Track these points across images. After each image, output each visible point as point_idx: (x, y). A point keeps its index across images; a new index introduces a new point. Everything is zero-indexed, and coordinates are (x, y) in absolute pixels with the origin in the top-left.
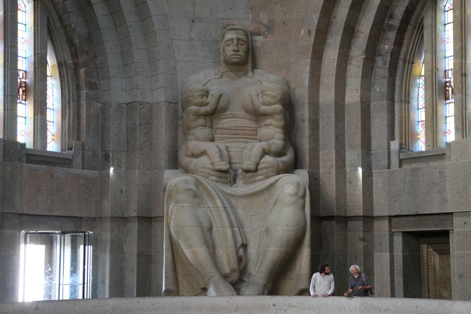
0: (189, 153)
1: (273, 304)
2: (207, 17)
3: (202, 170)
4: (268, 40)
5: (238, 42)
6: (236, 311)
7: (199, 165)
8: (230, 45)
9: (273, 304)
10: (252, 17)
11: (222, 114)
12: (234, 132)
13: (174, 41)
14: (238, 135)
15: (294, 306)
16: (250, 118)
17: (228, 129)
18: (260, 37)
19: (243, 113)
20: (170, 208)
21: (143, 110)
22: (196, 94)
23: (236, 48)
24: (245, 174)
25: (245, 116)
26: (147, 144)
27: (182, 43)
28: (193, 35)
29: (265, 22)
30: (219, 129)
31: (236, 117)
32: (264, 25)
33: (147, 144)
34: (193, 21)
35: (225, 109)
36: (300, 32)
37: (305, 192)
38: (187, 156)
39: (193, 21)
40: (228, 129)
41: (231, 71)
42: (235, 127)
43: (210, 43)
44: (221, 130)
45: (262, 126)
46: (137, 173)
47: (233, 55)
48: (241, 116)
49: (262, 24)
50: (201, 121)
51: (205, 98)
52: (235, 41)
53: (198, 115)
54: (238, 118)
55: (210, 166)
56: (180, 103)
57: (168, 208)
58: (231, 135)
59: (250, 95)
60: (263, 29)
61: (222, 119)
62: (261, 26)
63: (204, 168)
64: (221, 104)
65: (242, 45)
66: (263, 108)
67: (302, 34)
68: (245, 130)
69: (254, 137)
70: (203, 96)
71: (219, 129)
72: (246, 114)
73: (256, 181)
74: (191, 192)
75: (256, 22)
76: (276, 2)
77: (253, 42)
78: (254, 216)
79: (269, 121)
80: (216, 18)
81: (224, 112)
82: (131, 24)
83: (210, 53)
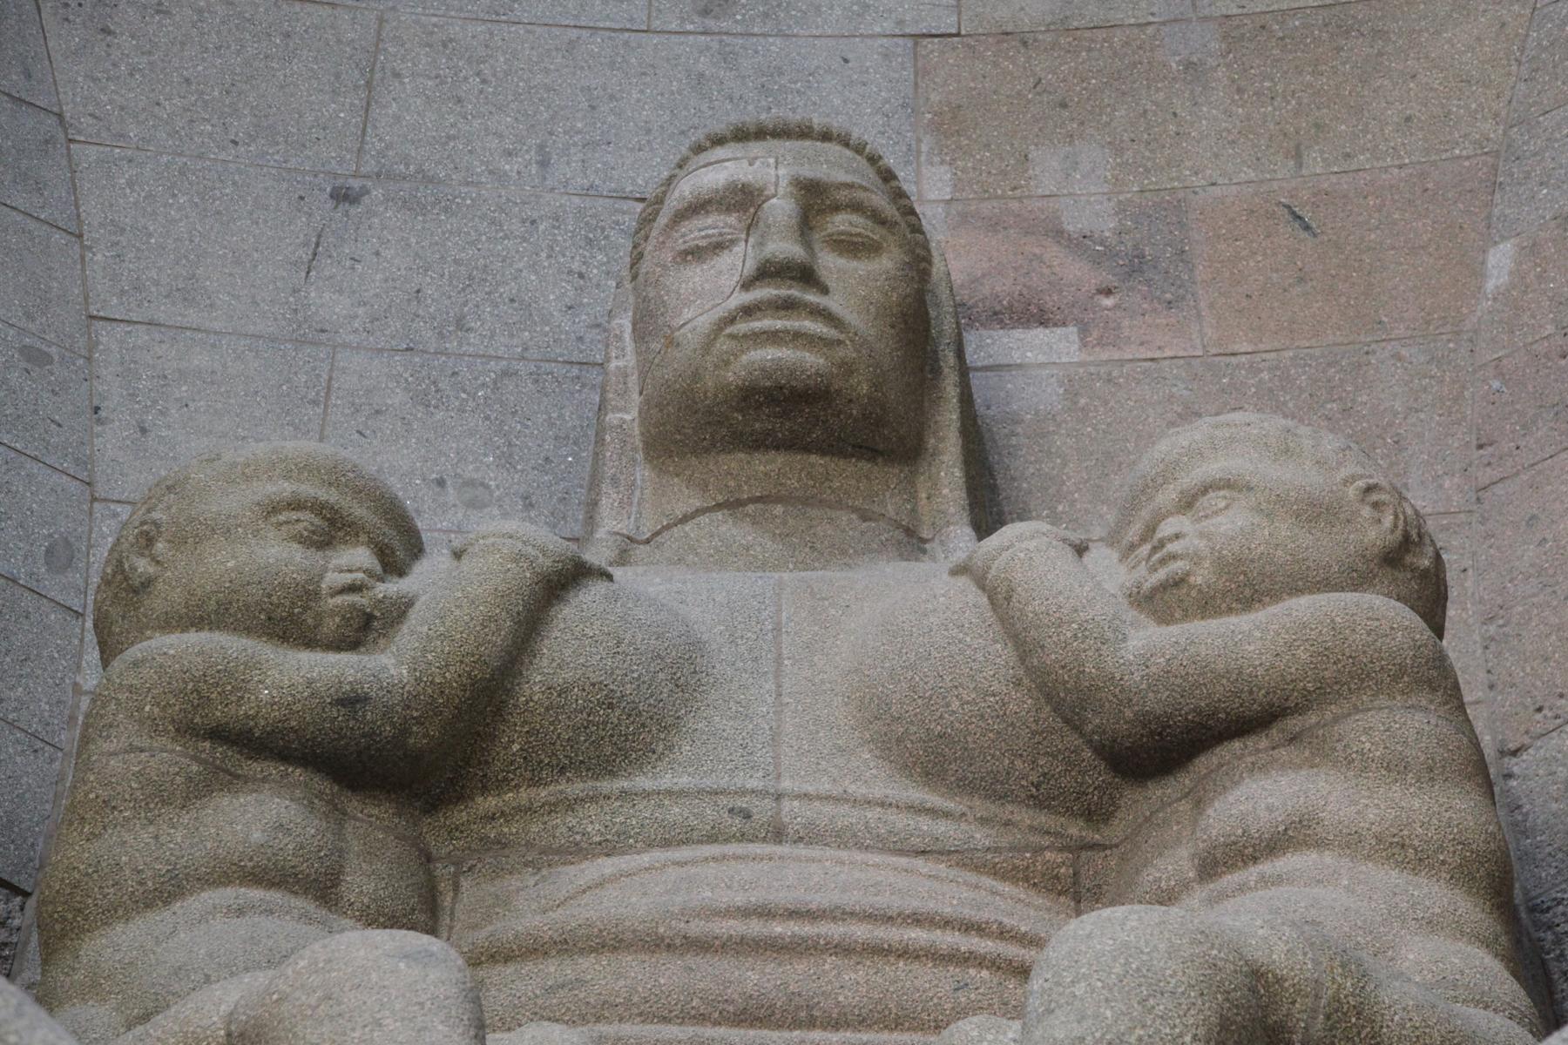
2: (499, 176)
5: (806, 224)
8: (719, 247)
10: (957, 185)
11: (576, 788)
12: (755, 978)
13: (107, 336)
16: (982, 837)
17: (654, 944)
18: (1039, 335)
19: (878, 781)
22: (236, 501)
23: (785, 247)
25: (901, 821)
28: (330, 304)
30: (534, 949)
31: (778, 834)
32: (1080, 244)
35: (617, 734)
36: (1478, 272)
40: (654, 944)
41: (732, 505)
43: (505, 373)
44: (553, 969)
47: (748, 311)
48: (847, 816)
49: (1059, 234)
50: (266, 813)
51: (357, 557)
52: (781, 208)
53: (241, 742)
54: (810, 836)
58: (702, 1019)
60: (1077, 272)
61: (578, 851)
62: (1054, 253)
64: (577, 642)
65: (850, 246)
66: (1148, 653)
68: (906, 953)
70: (331, 528)
71: (534, 949)
72: (917, 794)
75: (994, 225)
77: (976, 380)
79: (1255, 791)
80: (589, 192)
81: (606, 767)
83: (507, 461)
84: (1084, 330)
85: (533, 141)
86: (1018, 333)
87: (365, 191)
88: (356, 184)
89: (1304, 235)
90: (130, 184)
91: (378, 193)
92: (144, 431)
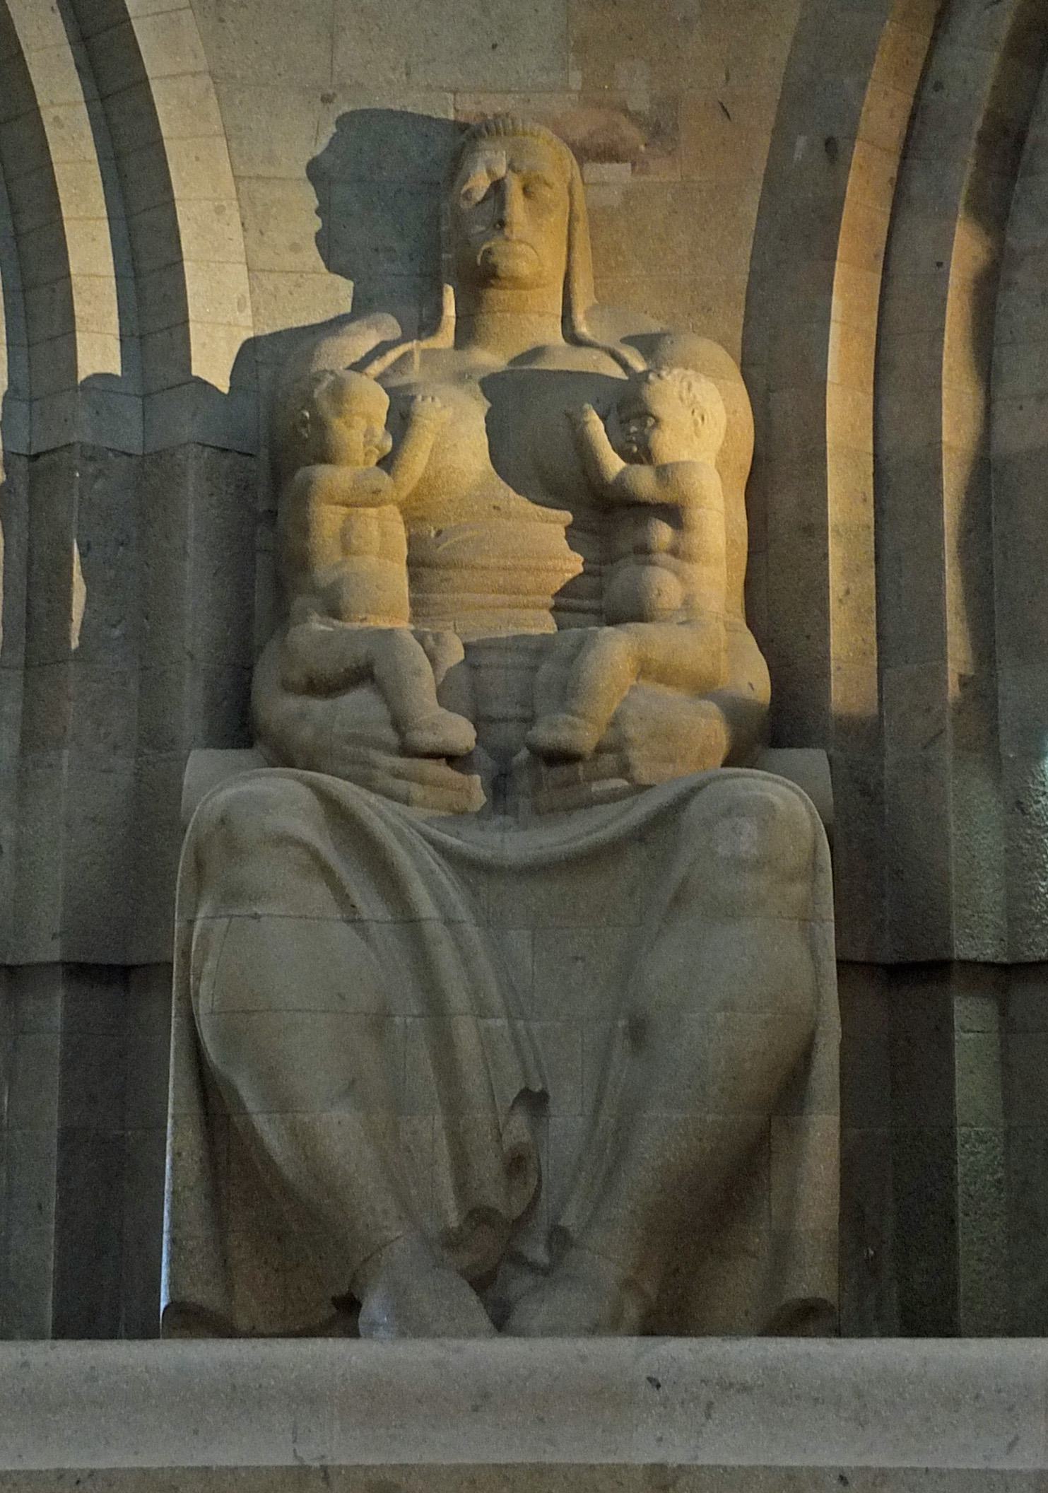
0: (296, 675)
1: (650, 1379)
2: (390, 82)
3: (349, 749)
6: (476, 1409)
7: (337, 728)
9: (650, 1379)
10: (585, 81)
14: (517, 591)
15: (745, 1389)
20: (198, 924)
21: (98, 486)
24: (543, 769)
26: (117, 632)
29: (640, 102)
32: (634, 117)
33: (117, 632)
34: (326, 99)
36: (793, 145)
37: (815, 850)
38: (288, 687)
39: (326, 99)
45: (622, 556)
46: (65, 762)
49: (625, 111)
55: (388, 735)
56: (264, 454)
57: (191, 922)
59: (568, 415)
60: (632, 134)
62: (623, 120)
63: (354, 739)
67: (797, 156)
69: (587, 603)
73: (590, 803)
74: (294, 852)
75: (599, 105)
76: (685, 19)
78: (579, 963)
82: (60, 112)
84: (634, 165)
85: (403, 61)
86: (607, 165)
88: (330, 91)
89: (726, 119)
90: (241, 103)
91: (340, 96)
92: (262, 233)
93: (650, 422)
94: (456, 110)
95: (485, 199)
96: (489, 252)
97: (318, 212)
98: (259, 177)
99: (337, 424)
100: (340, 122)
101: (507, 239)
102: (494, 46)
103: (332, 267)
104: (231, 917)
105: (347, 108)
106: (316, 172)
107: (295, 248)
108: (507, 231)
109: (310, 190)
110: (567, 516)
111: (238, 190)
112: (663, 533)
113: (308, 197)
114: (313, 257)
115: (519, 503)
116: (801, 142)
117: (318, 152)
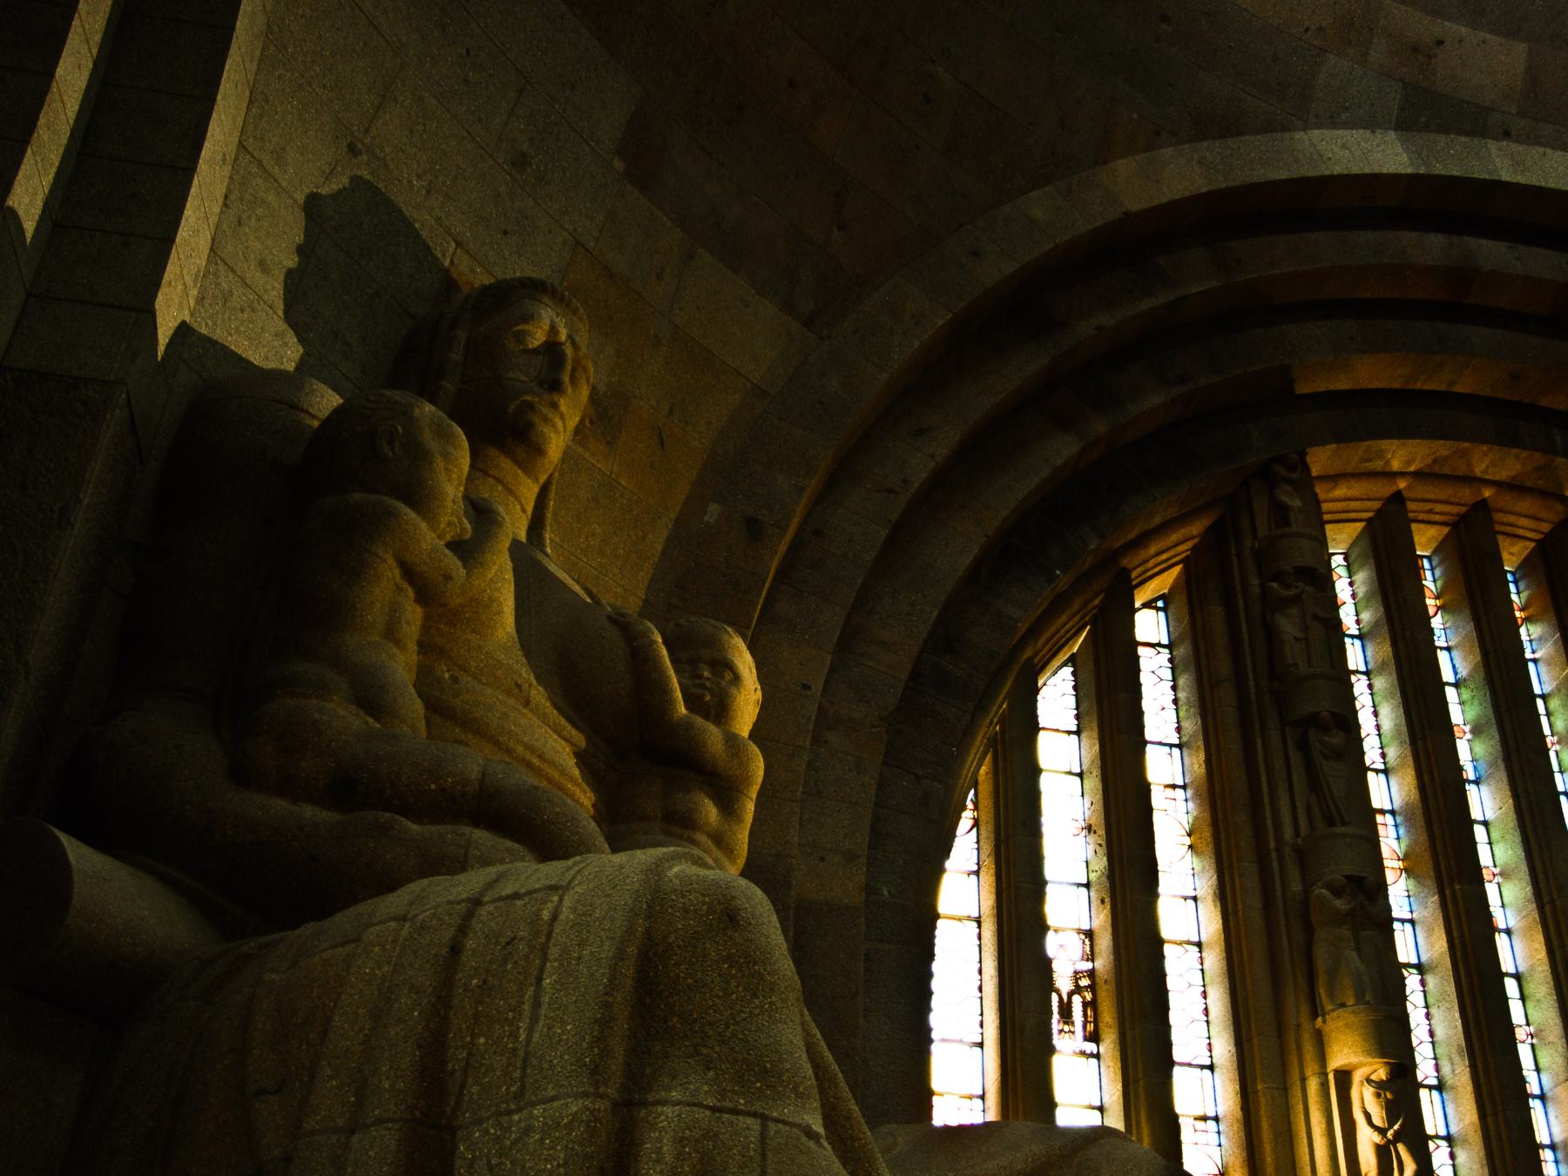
4: (587, 455)
27: (271, 198)
34: (353, 150)
42: (530, 748)
87: (360, 153)
88: (360, 146)
93: (728, 676)
94: (452, 262)
95: (535, 351)
96: (530, 407)
97: (300, 250)
98: (260, 164)
99: (439, 463)
100: (356, 180)
101: (555, 406)
102: (505, 233)
103: (288, 316)
104: (764, 1118)
105: (366, 175)
106: (313, 206)
107: (263, 266)
108: (555, 397)
109: (301, 216)
110: (580, 739)
111: (236, 159)
112: (710, 812)
113: (294, 230)
114: (275, 291)
115: (538, 694)
116: (713, 511)
117: (324, 191)
